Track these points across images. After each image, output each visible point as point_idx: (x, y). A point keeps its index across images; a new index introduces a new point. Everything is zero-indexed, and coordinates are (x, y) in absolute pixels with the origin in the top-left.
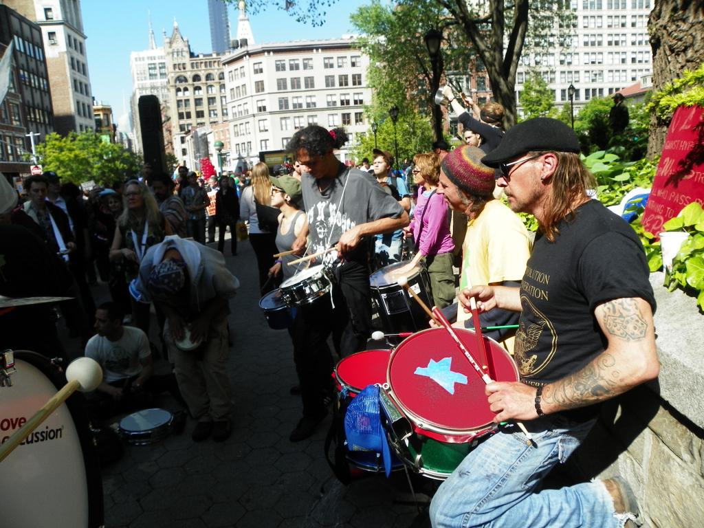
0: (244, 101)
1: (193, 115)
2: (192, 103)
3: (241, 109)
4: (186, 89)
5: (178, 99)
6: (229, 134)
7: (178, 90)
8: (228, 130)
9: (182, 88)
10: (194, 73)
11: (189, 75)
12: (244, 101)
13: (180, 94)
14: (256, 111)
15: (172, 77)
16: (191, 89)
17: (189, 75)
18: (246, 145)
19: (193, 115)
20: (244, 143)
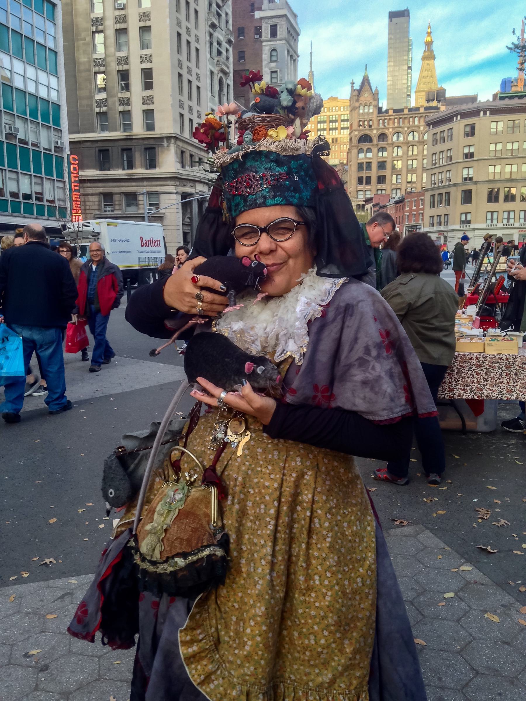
0: (448, 168)
1: (374, 180)
2: (374, 166)
3: (443, 176)
4: (369, 150)
5: (360, 161)
6: (423, 205)
7: (360, 151)
8: (423, 200)
9: (365, 149)
10: (380, 132)
11: (374, 133)
12: (448, 168)
13: (361, 156)
14: (460, 181)
15: (356, 136)
16: (375, 150)
17: (374, 133)
18: (435, 218)
19: (374, 180)
20: (440, 216)
